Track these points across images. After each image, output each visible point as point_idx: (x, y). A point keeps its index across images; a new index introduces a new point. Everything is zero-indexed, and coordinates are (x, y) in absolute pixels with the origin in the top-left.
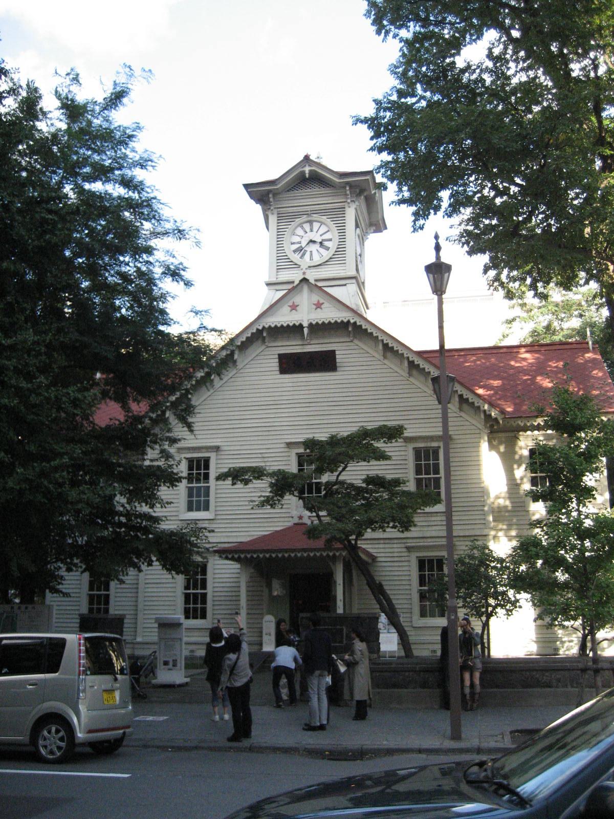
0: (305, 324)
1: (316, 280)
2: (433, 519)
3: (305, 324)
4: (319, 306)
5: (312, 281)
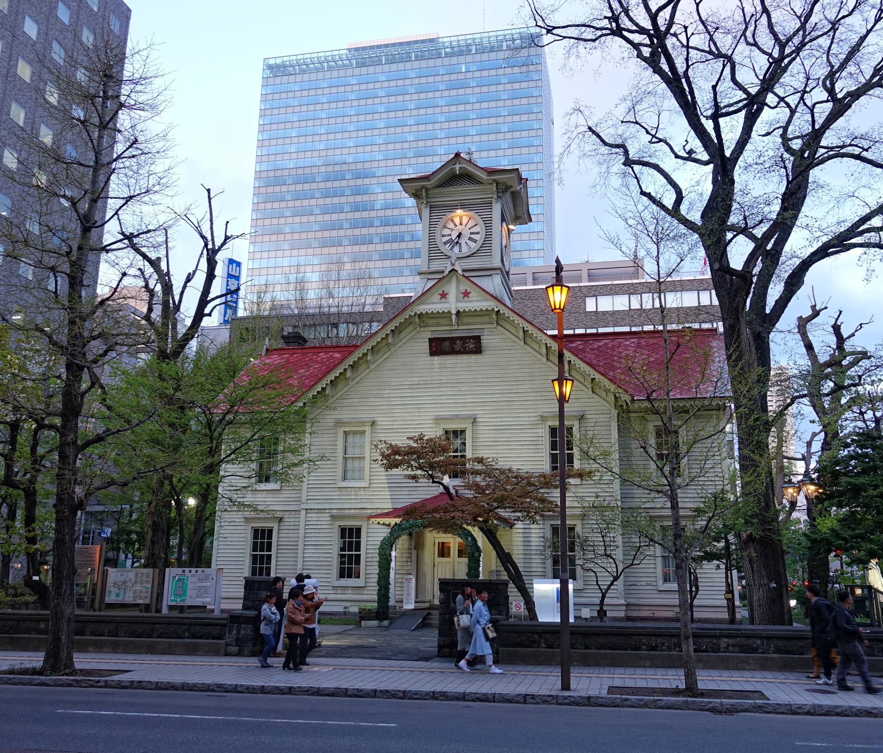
1: (463, 271)
3: (454, 312)
5: (460, 272)
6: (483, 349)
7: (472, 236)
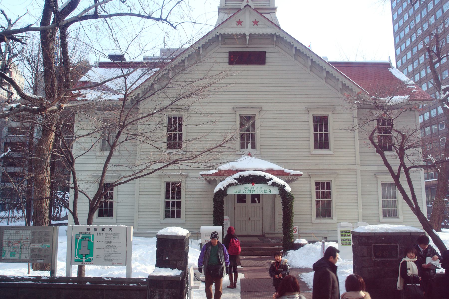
0: (248, 34)
2: (325, 158)
3: (248, 34)
4: (256, 23)
6: (266, 61)
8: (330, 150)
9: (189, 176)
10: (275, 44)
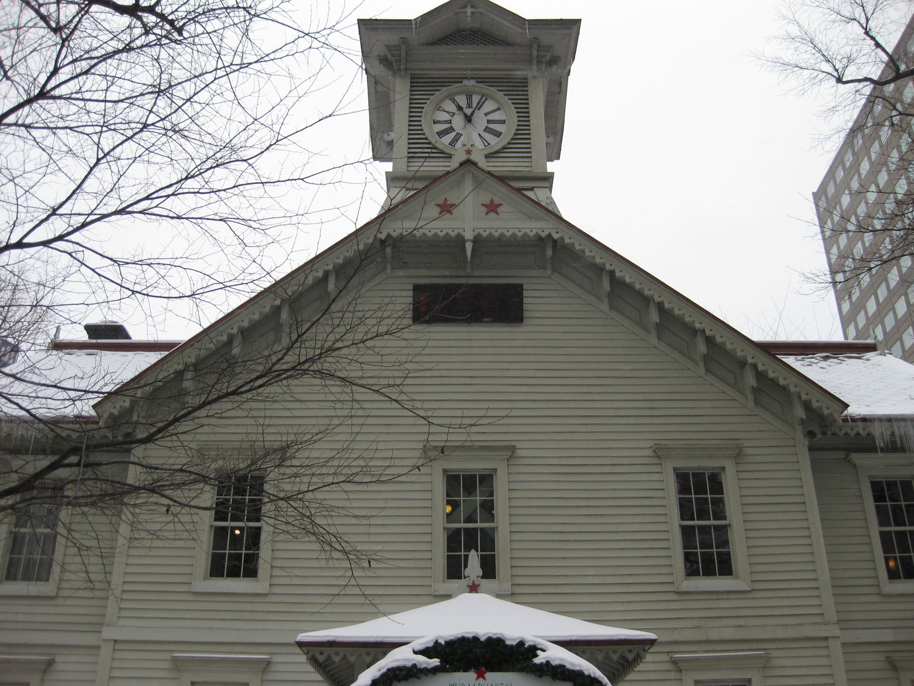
0: (469, 235)
3: (469, 235)
4: (492, 208)
5: (483, 163)
7: (492, 126)
8: (737, 577)
9: (274, 668)
10: (549, 266)
